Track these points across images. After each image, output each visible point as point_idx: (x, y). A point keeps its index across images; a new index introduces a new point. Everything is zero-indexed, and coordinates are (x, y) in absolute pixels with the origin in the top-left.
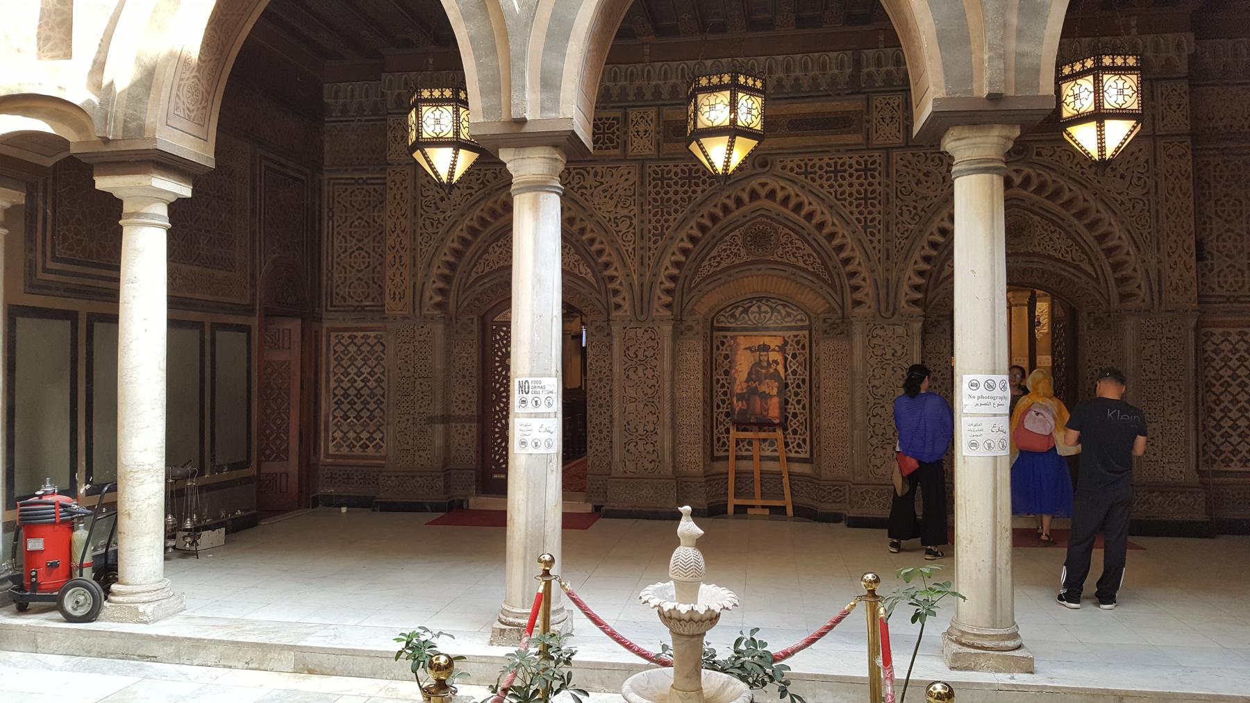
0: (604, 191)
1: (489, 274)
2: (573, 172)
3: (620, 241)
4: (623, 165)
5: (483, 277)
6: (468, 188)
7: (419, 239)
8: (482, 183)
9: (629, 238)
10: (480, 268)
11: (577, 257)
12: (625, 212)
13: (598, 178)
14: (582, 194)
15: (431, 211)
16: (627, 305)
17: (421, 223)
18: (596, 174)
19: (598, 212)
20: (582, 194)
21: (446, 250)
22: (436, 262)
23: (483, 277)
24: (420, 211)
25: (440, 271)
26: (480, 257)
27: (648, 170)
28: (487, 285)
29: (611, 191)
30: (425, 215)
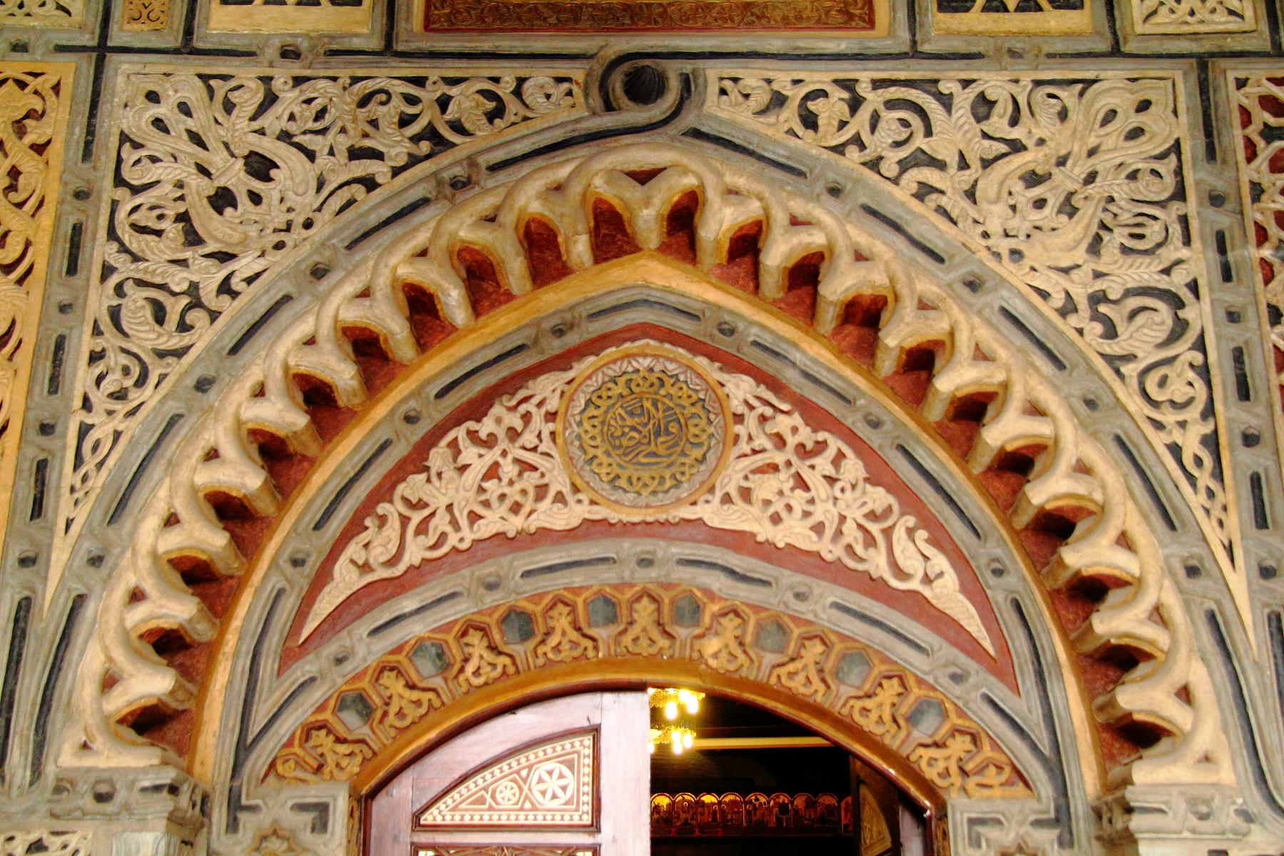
0: (1033, 179)
1: (416, 576)
2: (874, 99)
3: (1136, 405)
4: (1113, 75)
5: (398, 586)
6: (355, 154)
7: (80, 377)
8: (431, 134)
9: (1178, 390)
10: (378, 544)
11: (879, 497)
12: (1145, 272)
13: (998, 123)
14: (924, 191)
15: (158, 254)
16: (1207, 727)
17: (98, 301)
18: (983, 106)
19: (1007, 269)
20: (924, 191)
21: (220, 434)
22: (162, 493)
23: (398, 586)
24: (100, 250)
25: (173, 542)
26: (384, 491)
27: (1238, 97)
28: (416, 629)
29: (1067, 180)
30: (125, 268)
